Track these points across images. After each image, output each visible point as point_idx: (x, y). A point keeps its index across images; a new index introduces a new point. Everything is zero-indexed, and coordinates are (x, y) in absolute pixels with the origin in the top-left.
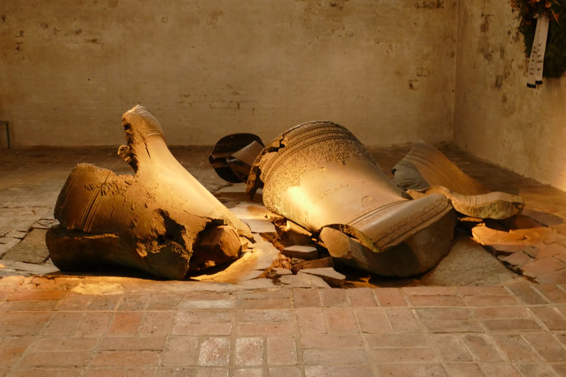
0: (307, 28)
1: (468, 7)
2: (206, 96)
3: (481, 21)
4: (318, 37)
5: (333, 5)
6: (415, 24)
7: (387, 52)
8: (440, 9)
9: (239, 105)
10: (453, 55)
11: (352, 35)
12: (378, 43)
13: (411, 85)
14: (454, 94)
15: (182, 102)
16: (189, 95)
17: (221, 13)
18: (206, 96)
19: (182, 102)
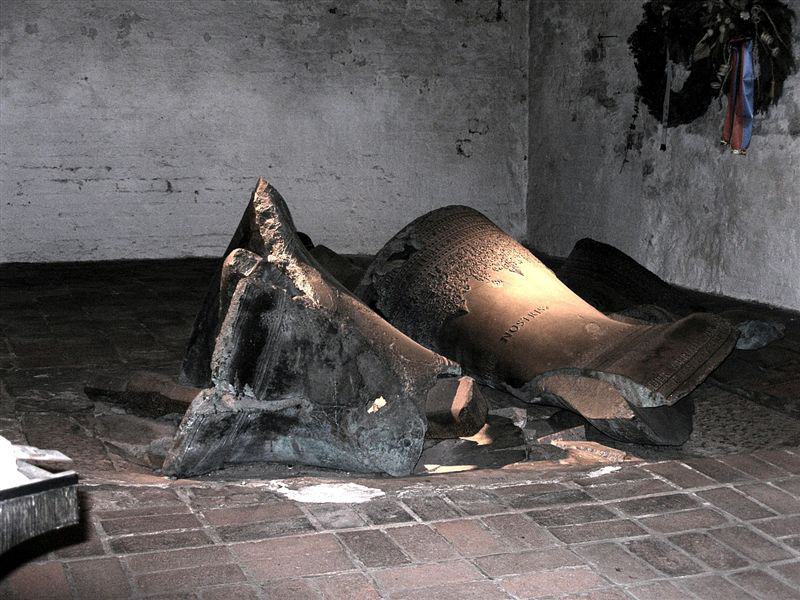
0: (288, 48)
1: (554, 21)
2: (109, 169)
3: (586, 45)
4: (307, 64)
5: (332, 11)
6: (464, 46)
7: (421, 92)
8: (502, 22)
9: (169, 185)
10: (523, 98)
11: (363, 63)
12: (406, 77)
13: (460, 151)
14: (527, 161)
15: (65, 181)
16: (77, 168)
17: (138, 19)
18: (109, 169)
19: (65, 181)
